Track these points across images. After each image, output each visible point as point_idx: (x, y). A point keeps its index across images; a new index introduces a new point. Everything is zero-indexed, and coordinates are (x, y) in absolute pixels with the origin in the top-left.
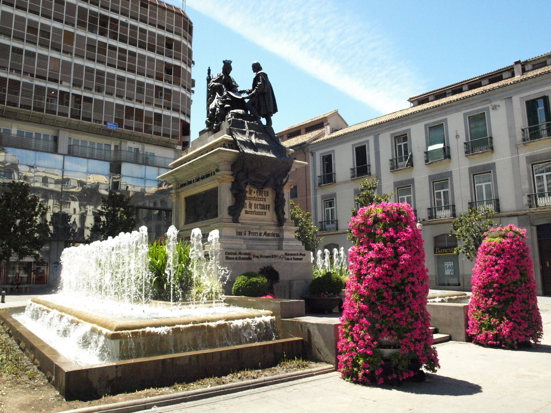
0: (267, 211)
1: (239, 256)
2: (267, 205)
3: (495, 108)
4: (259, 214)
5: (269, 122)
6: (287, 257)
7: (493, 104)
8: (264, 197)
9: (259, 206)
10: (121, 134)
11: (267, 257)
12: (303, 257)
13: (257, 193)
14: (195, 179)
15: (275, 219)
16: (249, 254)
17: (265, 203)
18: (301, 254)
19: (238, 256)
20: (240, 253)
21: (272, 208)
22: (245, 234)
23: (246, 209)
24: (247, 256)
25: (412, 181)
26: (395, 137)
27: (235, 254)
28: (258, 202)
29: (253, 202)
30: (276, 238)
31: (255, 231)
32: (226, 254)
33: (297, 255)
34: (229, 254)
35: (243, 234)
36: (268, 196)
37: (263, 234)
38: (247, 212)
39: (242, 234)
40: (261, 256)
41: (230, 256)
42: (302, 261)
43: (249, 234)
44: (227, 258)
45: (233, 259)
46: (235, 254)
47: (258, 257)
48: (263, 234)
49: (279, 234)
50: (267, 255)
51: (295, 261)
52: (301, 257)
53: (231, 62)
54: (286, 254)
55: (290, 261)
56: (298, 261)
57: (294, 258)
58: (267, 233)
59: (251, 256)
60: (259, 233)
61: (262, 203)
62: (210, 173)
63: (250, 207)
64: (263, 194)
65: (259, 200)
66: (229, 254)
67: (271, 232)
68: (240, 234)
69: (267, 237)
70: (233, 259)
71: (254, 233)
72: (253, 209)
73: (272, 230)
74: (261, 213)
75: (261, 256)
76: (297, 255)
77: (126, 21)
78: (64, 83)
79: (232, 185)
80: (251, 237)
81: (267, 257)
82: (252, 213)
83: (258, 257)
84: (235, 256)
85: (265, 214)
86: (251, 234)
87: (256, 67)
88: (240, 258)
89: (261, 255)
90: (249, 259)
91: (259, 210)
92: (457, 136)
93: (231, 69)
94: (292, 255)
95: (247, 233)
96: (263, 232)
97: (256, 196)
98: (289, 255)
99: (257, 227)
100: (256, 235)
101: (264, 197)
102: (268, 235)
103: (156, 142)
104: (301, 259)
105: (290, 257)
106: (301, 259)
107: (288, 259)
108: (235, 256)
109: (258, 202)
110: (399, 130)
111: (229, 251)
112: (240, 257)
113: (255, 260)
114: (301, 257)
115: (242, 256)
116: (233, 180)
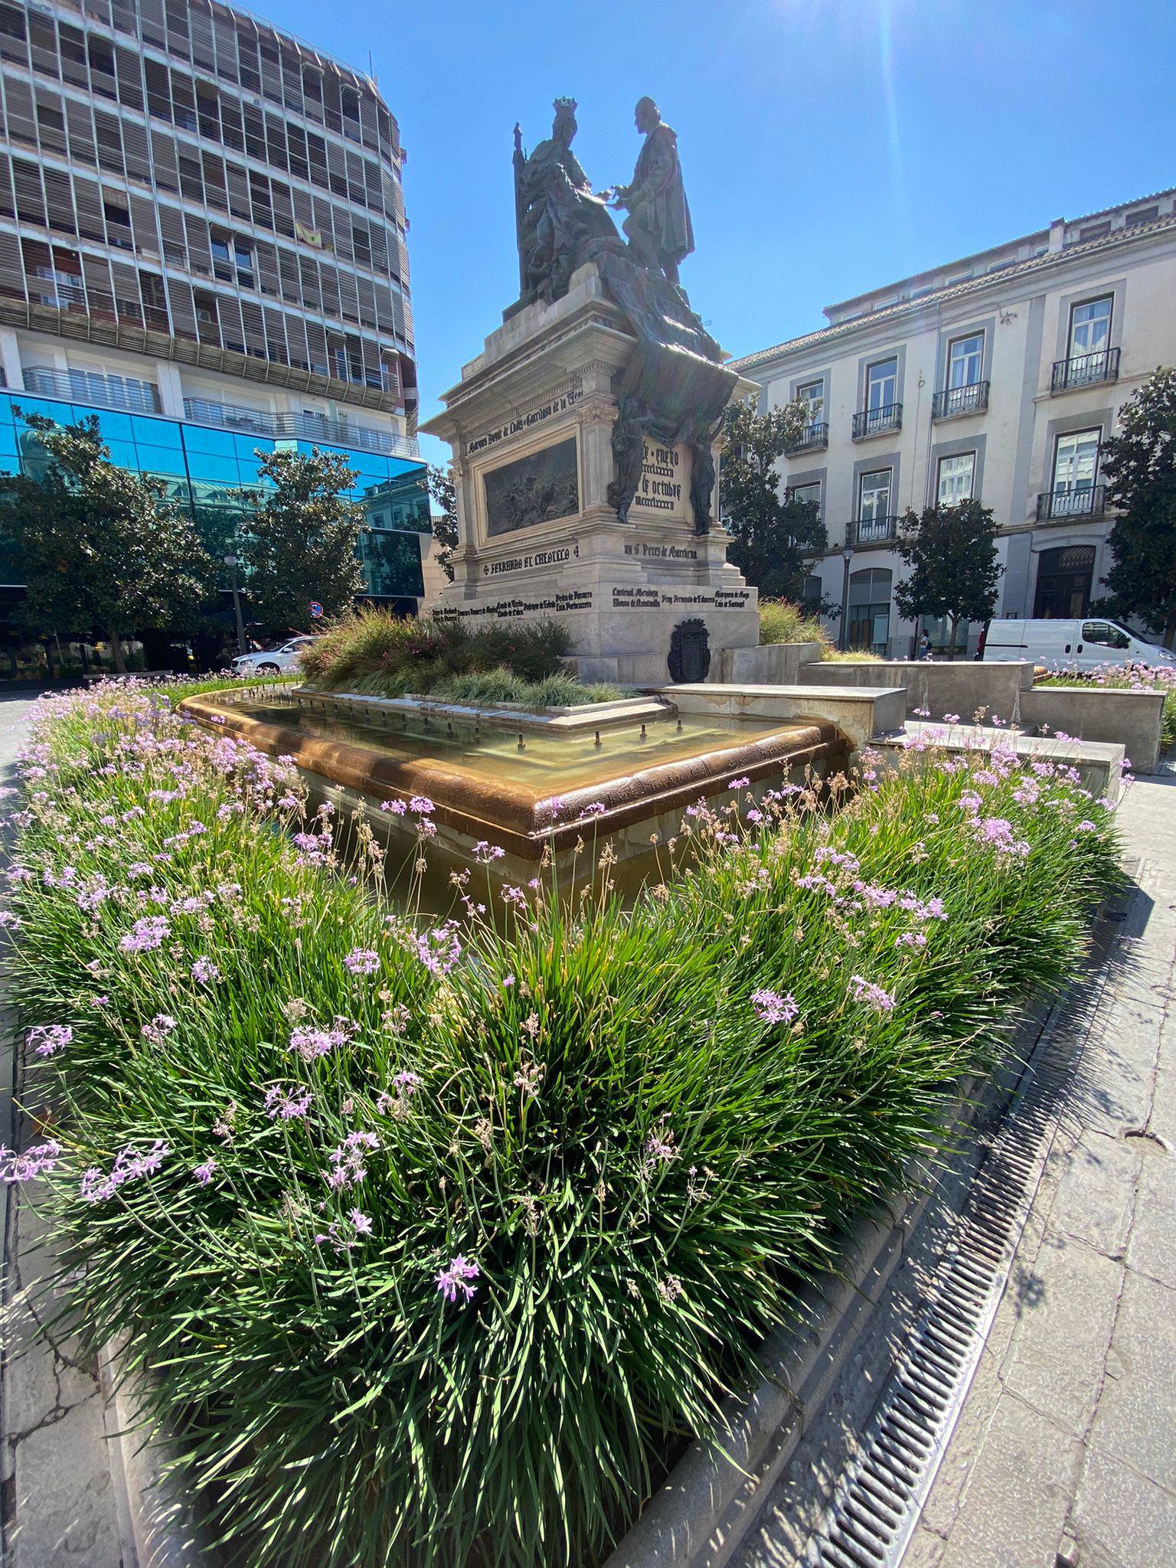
3: (1006, 320)
5: (673, 274)
6: (719, 600)
7: (1004, 311)
8: (670, 466)
10: (285, 377)
11: (684, 600)
14: (508, 426)
15: (690, 516)
16: (655, 593)
17: (673, 481)
19: (635, 599)
20: (639, 592)
21: (685, 492)
24: (651, 599)
25: (824, 471)
26: (799, 388)
27: (630, 593)
28: (658, 479)
29: (652, 477)
30: (690, 560)
31: (654, 545)
38: (639, 501)
41: (622, 598)
44: (617, 603)
45: (625, 604)
46: (630, 593)
47: (670, 600)
51: (731, 609)
52: (740, 600)
53: (575, 105)
54: (718, 594)
56: (738, 609)
59: (660, 600)
61: (666, 480)
62: (552, 405)
63: (645, 490)
66: (619, 593)
68: (628, 550)
70: (625, 604)
72: (651, 495)
73: (684, 542)
75: (677, 599)
77: (256, 101)
78: (145, 252)
79: (614, 431)
80: (647, 557)
81: (684, 600)
82: (648, 502)
83: (670, 600)
84: (629, 599)
87: (646, 115)
88: (639, 603)
90: (656, 604)
92: (921, 383)
93: (575, 128)
95: (641, 549)
96: (668, 547)
99: (659, 535)
101: (670, 466)
102: (677, 553)
104: (741, 605)
105: (724, 600)
106: (741, 605)
107: (721, 605)
108: (629, 599)
109: (658, 479)
110: (807, 374)
111: (620, 587)
113: (665, 605)
114: (740, 600)
116: (616, 418)
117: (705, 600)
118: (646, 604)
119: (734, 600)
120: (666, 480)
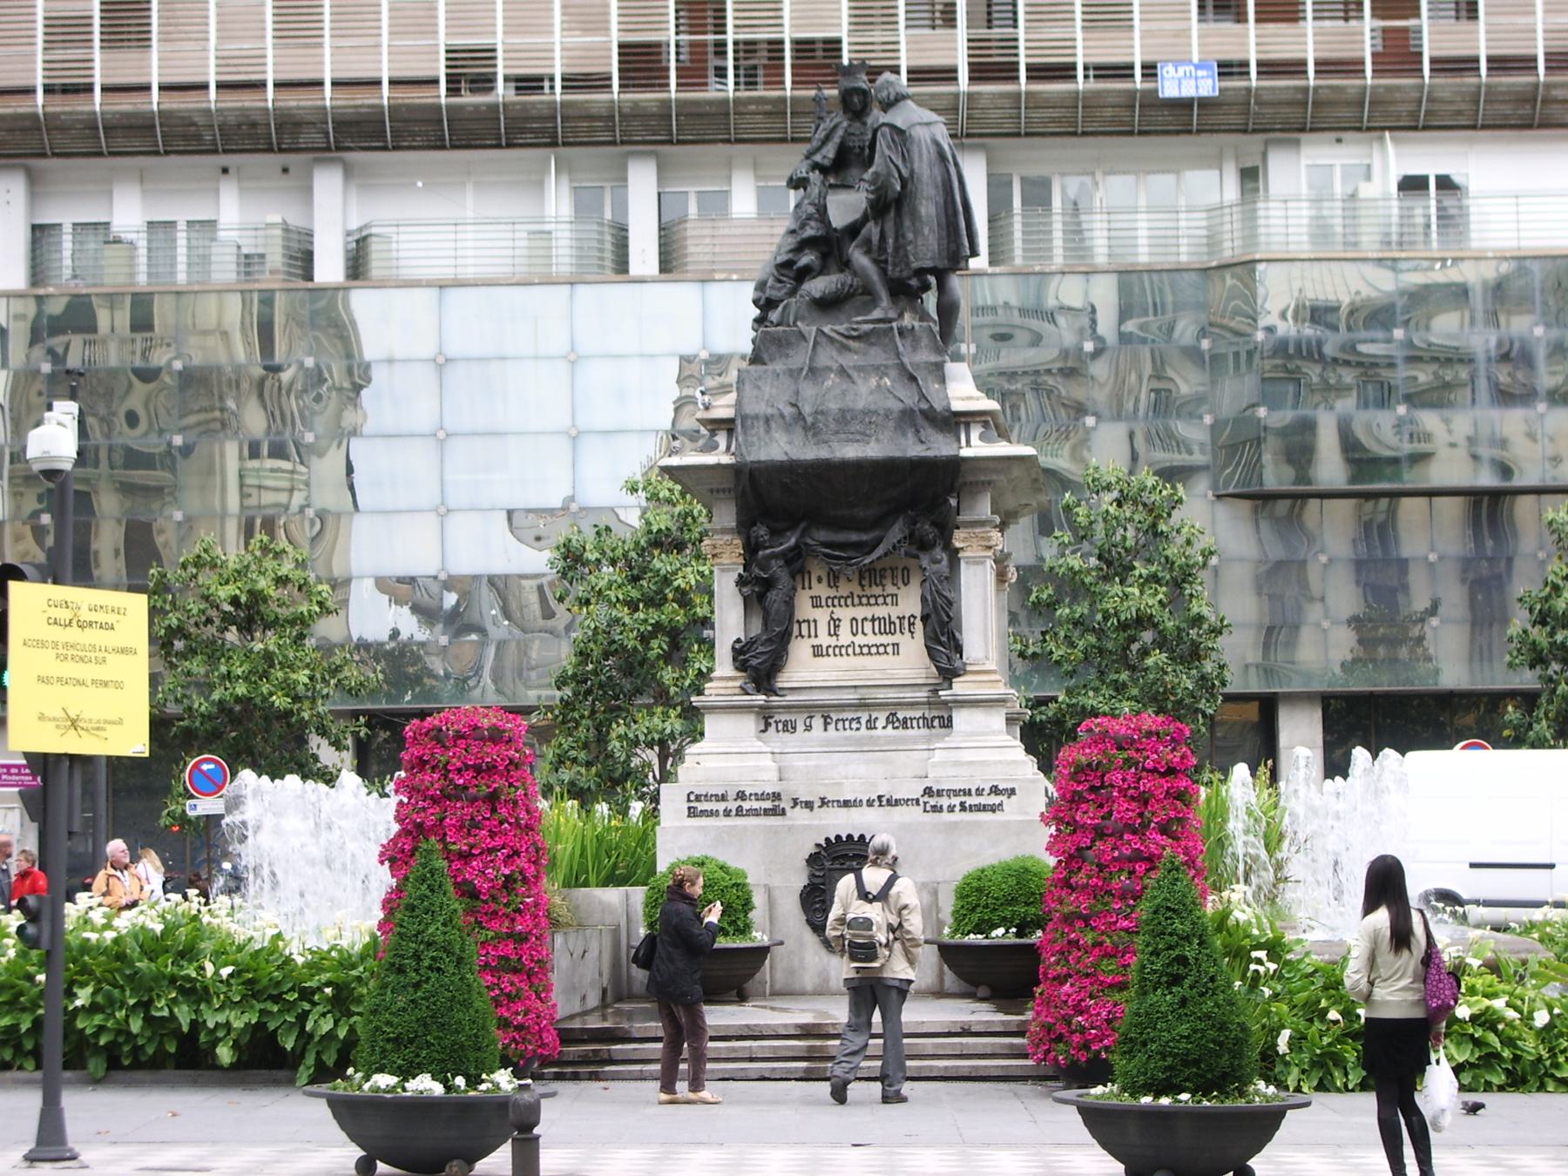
0: (903, 640)
1: (739, 803)
2: (901, 619)
4: (870, 653)
6: (932, 801)
8: (890, 589)
9: (868, 626)
11: (846, 804)
12: (1004, 798)
13: (861, 578)
16: (777, 796)
17: (894, 612)
18: (995, 790)
19: (733, 805)
20: (741, 796)
22: (809, 728)
27: (723, 798)
28: (861, 612)
29: (845, 614)
32: (689, 800)
33: (979, 792)
34: (698, 798)
35: (800, 727)
36: (905, 585)
37: (881, 723)
38: (818, 652)
39: (794, 728)
40: (824, 802)
41: (701, 806)
42: (998, 816)
43: (826, 724)
44: (692, 813)
46: (723, 798)
47: (809, 805)
48: (881, 723)
49: (950, 719)
50: (850, 797)
51: (967, 816)
52: (995, 800)
54: (928, 791)
55: (945, 816)
57: (962, 804)
58: (900, 715)
59: (785, 804)
60: (863, 721)
61: (881, 611)
64: (888, 582)
65: (869, 604)
66: (698, 798)
67: (918, 714)
69: (901, 732)
71: (843, 721)
74: (881, 650)
75: (824, 802)
76: (979, 792)
81: (846, 804)
82: (839, 650)
83: (809, 805)
84: (721, 806)
85: (896, 651)
86: (831, 727)
88: (740, 812)
89: (822, 799)
91: (871, 639)
94: (956, 793)
95: (818, 722)
96: (882, 717)
97: (858, 591)
98: (939, 793)
100: (854, 725)
103: (1459, 113)
105: (945, 802)
106: (993, 809)
107: (937, 809)
112: (739, 809)
114: (995, 800)
115: (746, 805)
117: (893, 803)
118: (754, 813)
120: (881, 611)
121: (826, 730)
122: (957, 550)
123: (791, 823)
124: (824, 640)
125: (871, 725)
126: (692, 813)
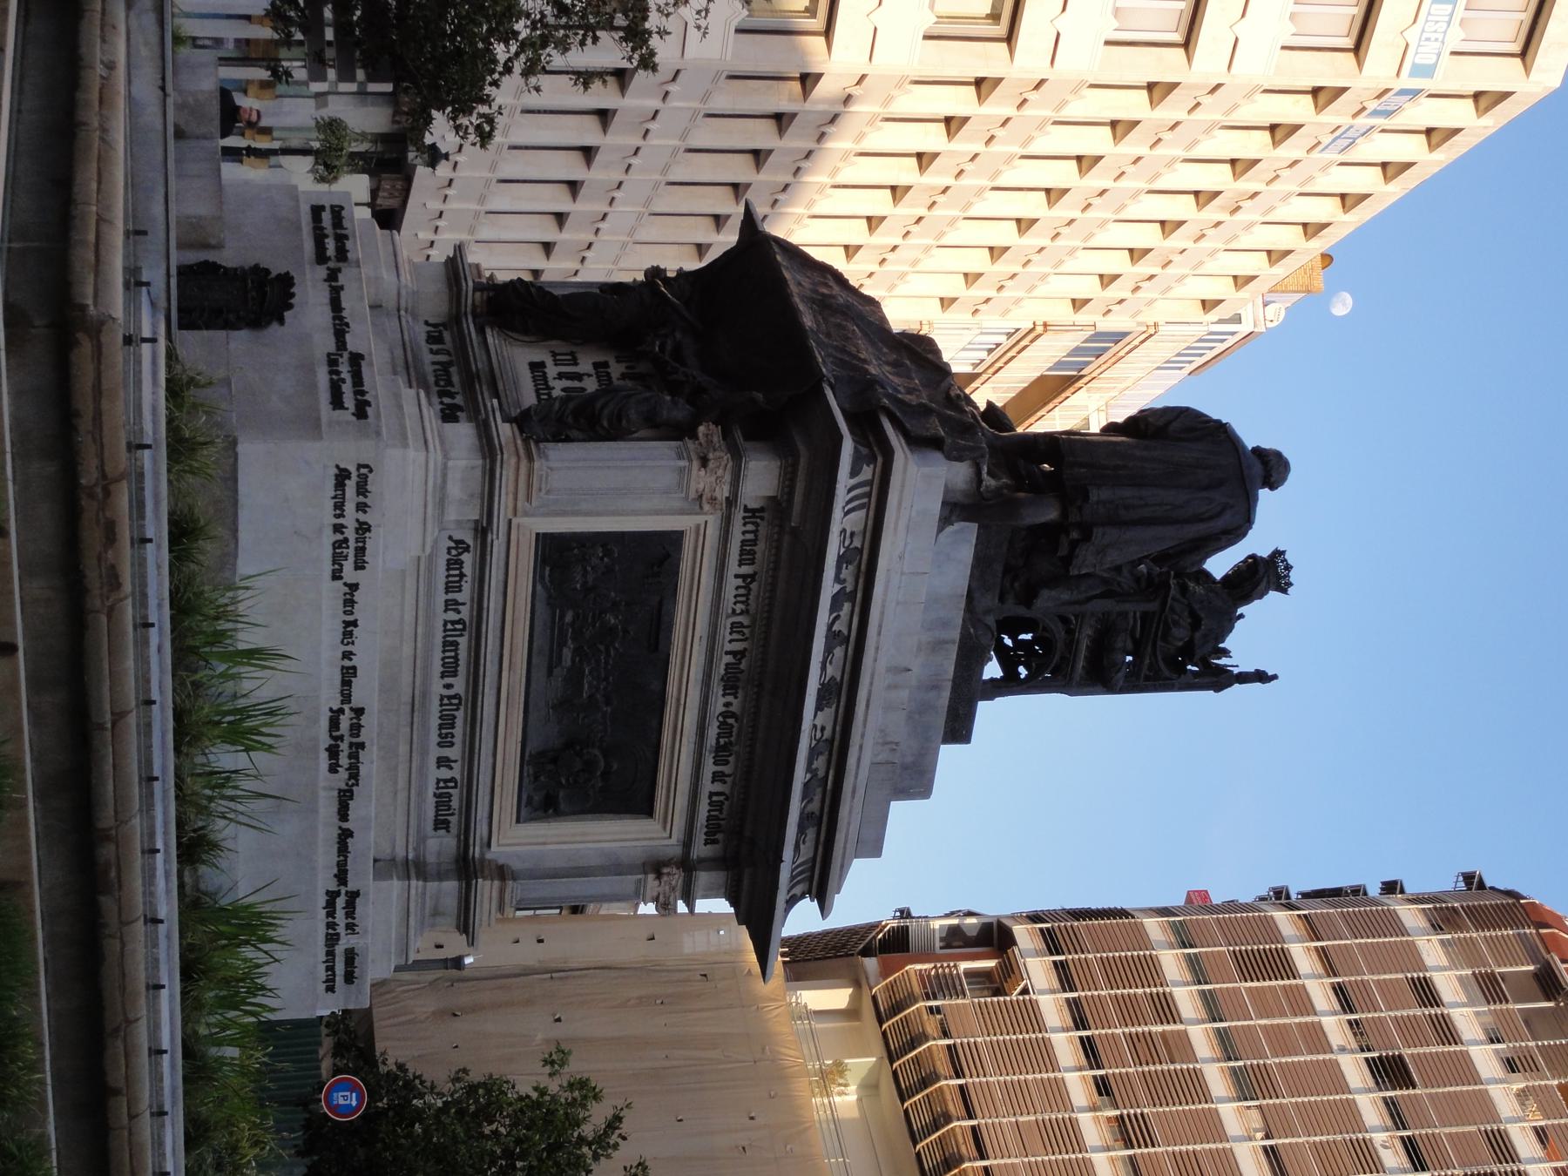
12: (352, 409)
19: (329, 229)
23: (549, 362)
31: (456, 379)
35: (435, 347)
37: (447, 400)
57: (343, 381)
59: (331, 264)
63: (561, 376)
86: (437, 367)
90: (321, 258)
95: (442, 358)
105: (344, 369)
106: (337, 402)
119: (347, 388)
121: (434, 363)
122: (694, 436)
123: (307, 267)
124: (552, 371)
125: (443, 762)
126: (317, 211)
